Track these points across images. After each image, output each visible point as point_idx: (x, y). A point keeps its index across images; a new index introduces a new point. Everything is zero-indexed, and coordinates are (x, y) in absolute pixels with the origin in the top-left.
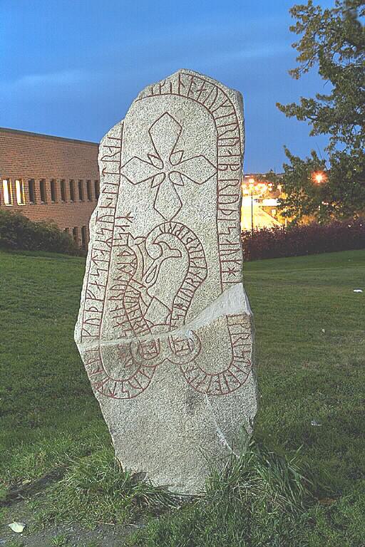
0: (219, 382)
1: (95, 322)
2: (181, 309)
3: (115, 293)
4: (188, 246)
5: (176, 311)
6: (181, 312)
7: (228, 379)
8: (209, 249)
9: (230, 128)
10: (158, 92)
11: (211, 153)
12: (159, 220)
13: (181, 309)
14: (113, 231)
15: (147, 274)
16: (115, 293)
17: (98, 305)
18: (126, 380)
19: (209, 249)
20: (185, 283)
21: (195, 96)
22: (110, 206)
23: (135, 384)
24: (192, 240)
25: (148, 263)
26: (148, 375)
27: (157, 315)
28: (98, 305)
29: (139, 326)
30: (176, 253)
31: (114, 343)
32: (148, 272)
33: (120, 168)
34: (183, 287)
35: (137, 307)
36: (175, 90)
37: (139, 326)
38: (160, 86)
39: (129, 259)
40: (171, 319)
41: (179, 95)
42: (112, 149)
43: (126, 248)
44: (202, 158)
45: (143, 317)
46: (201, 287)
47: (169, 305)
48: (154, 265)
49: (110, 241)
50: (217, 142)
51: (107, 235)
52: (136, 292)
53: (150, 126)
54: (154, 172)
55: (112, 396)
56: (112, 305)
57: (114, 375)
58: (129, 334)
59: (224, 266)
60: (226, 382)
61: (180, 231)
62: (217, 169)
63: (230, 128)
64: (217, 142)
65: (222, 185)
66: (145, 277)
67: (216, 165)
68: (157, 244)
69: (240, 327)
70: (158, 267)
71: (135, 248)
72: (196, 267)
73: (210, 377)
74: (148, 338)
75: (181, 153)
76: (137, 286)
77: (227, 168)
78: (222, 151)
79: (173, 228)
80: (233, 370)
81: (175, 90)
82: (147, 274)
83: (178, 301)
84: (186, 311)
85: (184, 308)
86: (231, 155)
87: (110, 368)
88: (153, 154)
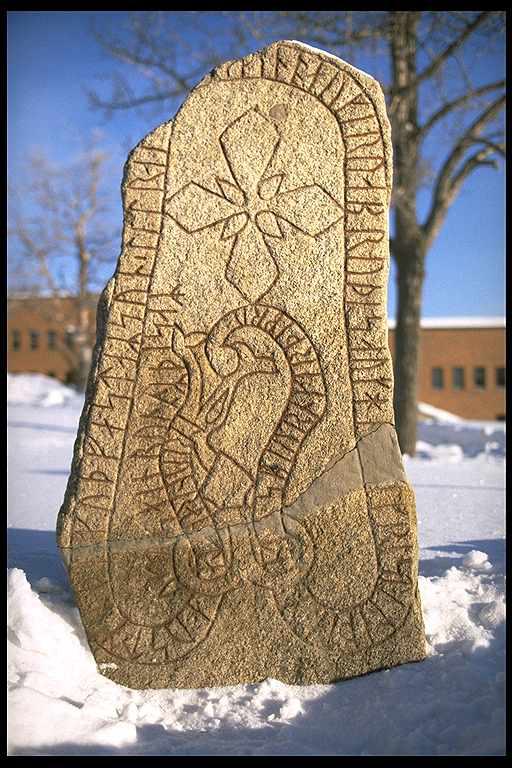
5: (269, 481)
51: (135, 327)
74: (204, 537)
76: (188, 429)
77: (362, 210)
88: (226, 178)
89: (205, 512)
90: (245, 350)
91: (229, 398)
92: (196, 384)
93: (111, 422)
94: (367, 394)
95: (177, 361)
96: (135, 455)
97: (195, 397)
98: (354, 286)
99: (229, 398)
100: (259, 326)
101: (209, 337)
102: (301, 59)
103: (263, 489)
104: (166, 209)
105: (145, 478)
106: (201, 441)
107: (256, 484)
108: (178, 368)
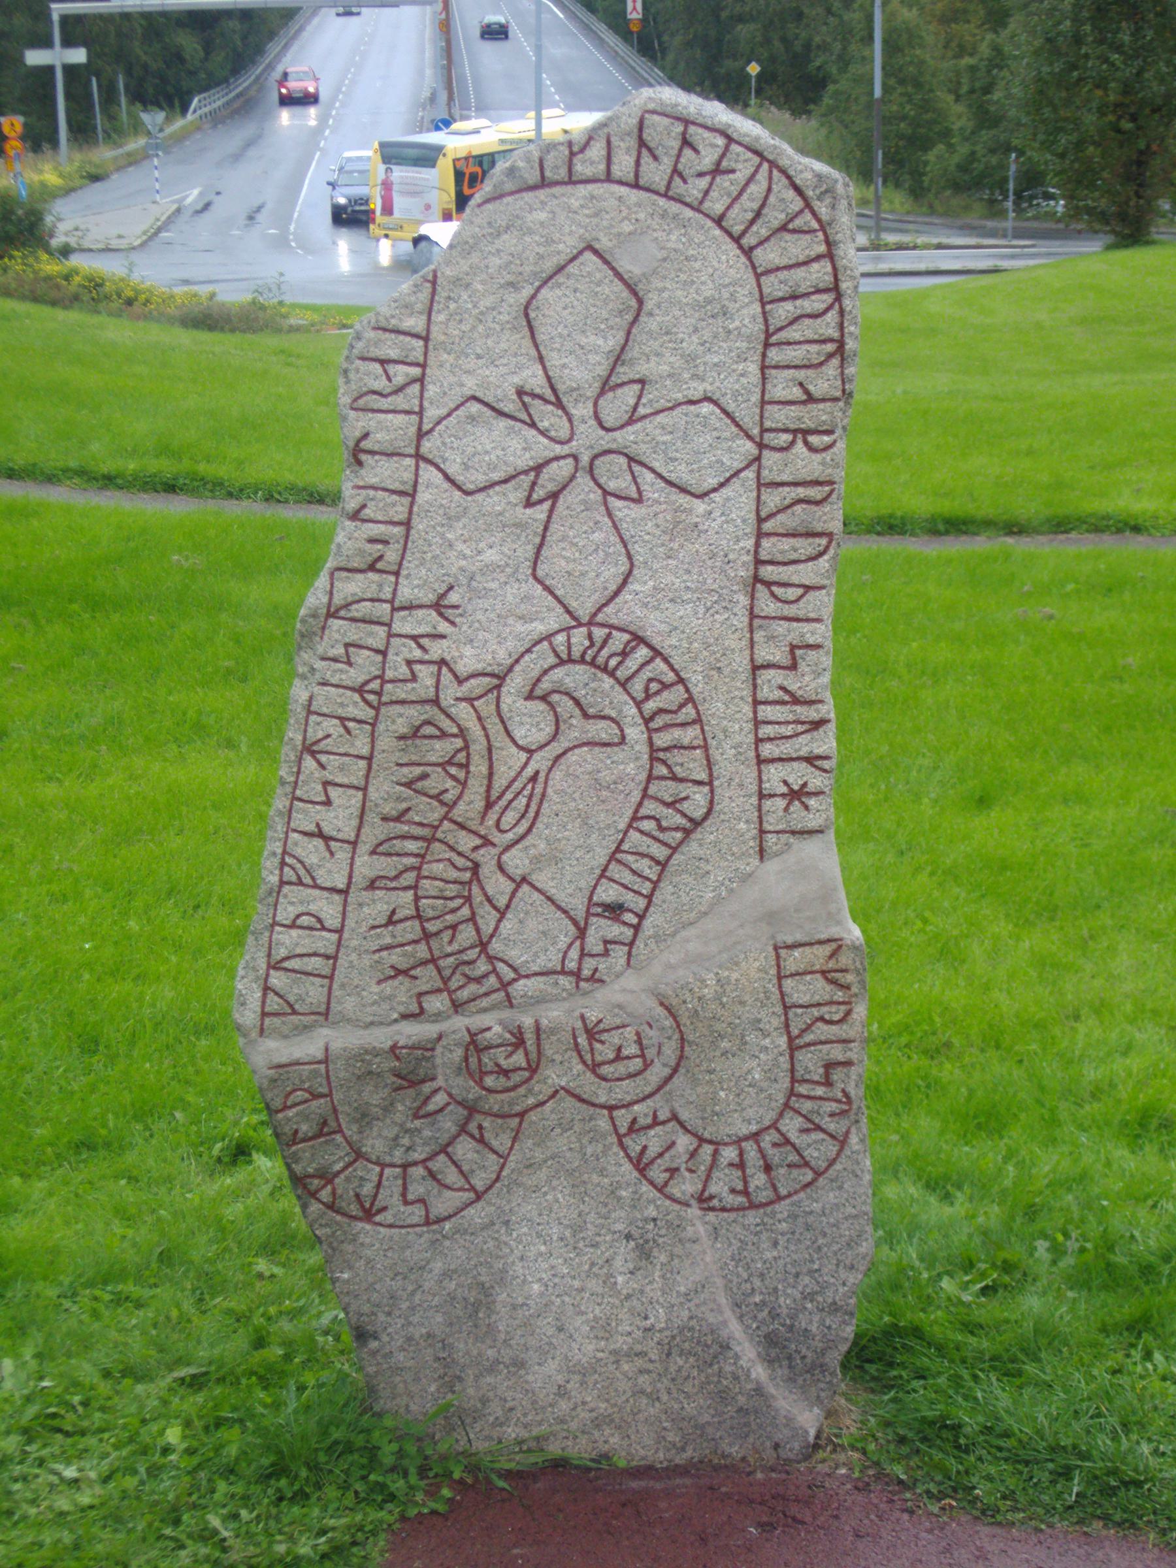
0: (741, 1165)
1: (315, 963)
2: (614, 917)
3: (385, 866)
4: (651, 706)
5: (601, 929)
6: (615, 930)
7: (774, 1155)
8: (727, 713)
9: (807, 305)
10: (563, 173)
11: (737, 380)
12: (554, 619)
13: (614, 917)
14: (384, 653)
15: (503, 802)
16: (385, 866)
17: (329, 909)
18: (415, 1164)
19: (727, 713)
20: (634, 835)
21: (694, 189)
22: (379, 566)
23: (452, 1176)
24: (665, 686)
25: (510, 761)
26: (495, 1143)
27: (531, 938)
28: (329, 909)
29: (470, 979)
30: (602, 730)
31: (381, 1038)
32: (509, 796)
33: (421, 435)
34: (625, 847)
35: (465, 912)
36: (623, 164)
37: (470, 979)
38: (572, 154)
39: (440, 749)
40: (583, 954)
41: (636, 186)
42: (391, 369)
43: (431, 711)
44: (706, 408)
45: (483, 945)
46: (692, 848)
47: (578, 905)
48: (529, 771)
49: (375, 685)
50: (764, 355)
52: (460, 862)
53: (527, 291)
54: (543, 448)
55: (368, 1215)
56: (378, 905)
57: (374, 1145)
58: (436, 1003)
59: (774, 776)
60: (768, 1168)
61: (624, 654)
62: (761, 446)
63: (807, 305)
64: (764, 355)
65: (773, 499)
66: (491, 821)
67: (756, 431)
68: (544, 698)
69: (819, 982)
70: (542, 776)
71: (463, 712)
72: (674, 778)
73: (708, 1149)
75: (637, 387)
77: (793, 443)
78: (782, 386)
79: (603, 645)
80: (791, 1125)
81: (623, 164)
82: (503, 802)
83: (608, 893)
84: (637, 928)
85: (630, 918)
86: (810, 399)
87: (364, 1118)
88: (538, 391)
89: (492, 979)
90: (565, 706)
91: (539, 789)
92: (479, 767)
93: (327, 829)
94: (785, 782)
95: (446, 725)
96: (372, 885)
97: (476, 788)
98: (768, 584)
99: (539, 789)
100: (592, 663)
101: (500, 678)
102: (686, 142)
103: (593, 942)
104: (423, 450)
105: (390, 922)
106: (486, 857)
107: (582, 933)
108: (444, 735)
